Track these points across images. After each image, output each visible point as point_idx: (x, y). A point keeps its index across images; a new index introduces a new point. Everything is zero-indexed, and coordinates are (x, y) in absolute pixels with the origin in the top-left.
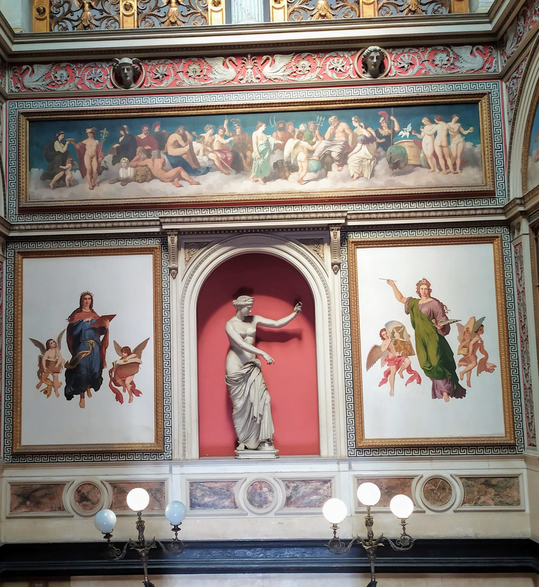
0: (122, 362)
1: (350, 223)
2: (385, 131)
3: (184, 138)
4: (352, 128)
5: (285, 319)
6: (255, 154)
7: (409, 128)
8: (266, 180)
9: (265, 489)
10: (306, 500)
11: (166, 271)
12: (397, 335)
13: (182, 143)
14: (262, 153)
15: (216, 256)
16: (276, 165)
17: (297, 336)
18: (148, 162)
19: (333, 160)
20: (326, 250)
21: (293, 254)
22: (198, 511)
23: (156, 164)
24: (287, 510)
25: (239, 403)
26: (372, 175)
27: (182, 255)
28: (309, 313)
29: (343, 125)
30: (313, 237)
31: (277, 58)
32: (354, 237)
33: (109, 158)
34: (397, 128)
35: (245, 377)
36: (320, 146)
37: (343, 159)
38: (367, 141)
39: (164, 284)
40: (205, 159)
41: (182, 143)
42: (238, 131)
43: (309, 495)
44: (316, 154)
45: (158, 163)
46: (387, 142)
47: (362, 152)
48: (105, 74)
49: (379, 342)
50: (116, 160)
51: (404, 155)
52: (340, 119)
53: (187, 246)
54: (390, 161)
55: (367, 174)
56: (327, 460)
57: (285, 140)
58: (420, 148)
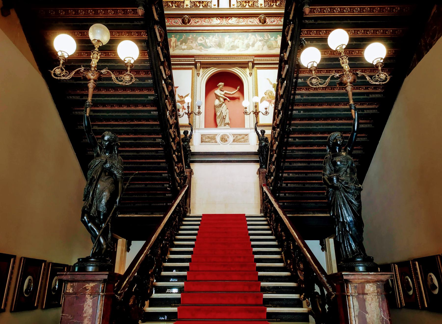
0: (180, 100)
1: (255, 62)
2: (266, 38)
3: (203, 38)
4: (256, 37)
5: (233, 92)
6: (225, 43)
7: (274, 37)
8: (229, 50)
9: (226, 137)
10: (240, 140)
11: (196, 74)
12: (270, 94)
13: (202, 39)
14: (228, 43)
15: (212, 71)
16: (232, 46)
17: (238, 98)
18: (191, 44)
19: (250, 45)
20: (247, 70)
21: (237, 71)
22: (203, 143)
23: (194, 45)
24: (233, 143)
25: (218, 114)
26: (262, 50)
27: (201, 70)
28: (242, 91)
29: (253, 36)
30: (243, 65)
31: (233, 18)
32: (256, 66)
33: (179, 43)
34: (270, 37)
35: (221, 105)
36: (246, 42)
37: (253, 45)
38: (260, 41)
39: (195, 79)
40: (210, 44)
41: (202, 39)
42: (220, 37)
43: (241, 139)
44: (245, 44)
45: (195, 45)
46: (267, 41)
47: (259, 44)
48: (179, 21)
49: (264, 96)
50: (181, 44)
51: (272, 45)
52: (252, 35)
53: (203, 68)
54: (268, 46)
55: (261, 49)
56: (247, 129)
57: (235, 40)
58: (277, 43)
